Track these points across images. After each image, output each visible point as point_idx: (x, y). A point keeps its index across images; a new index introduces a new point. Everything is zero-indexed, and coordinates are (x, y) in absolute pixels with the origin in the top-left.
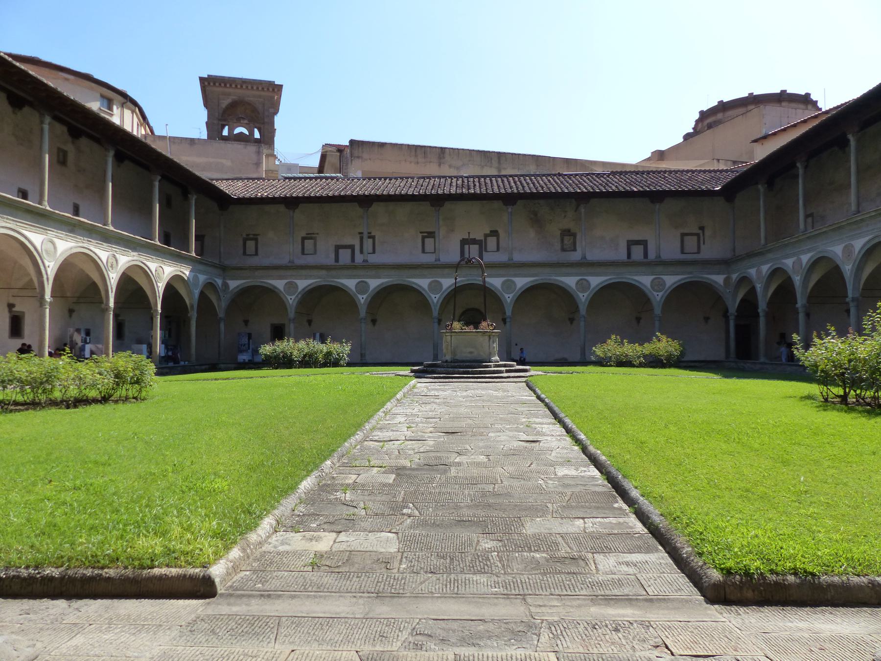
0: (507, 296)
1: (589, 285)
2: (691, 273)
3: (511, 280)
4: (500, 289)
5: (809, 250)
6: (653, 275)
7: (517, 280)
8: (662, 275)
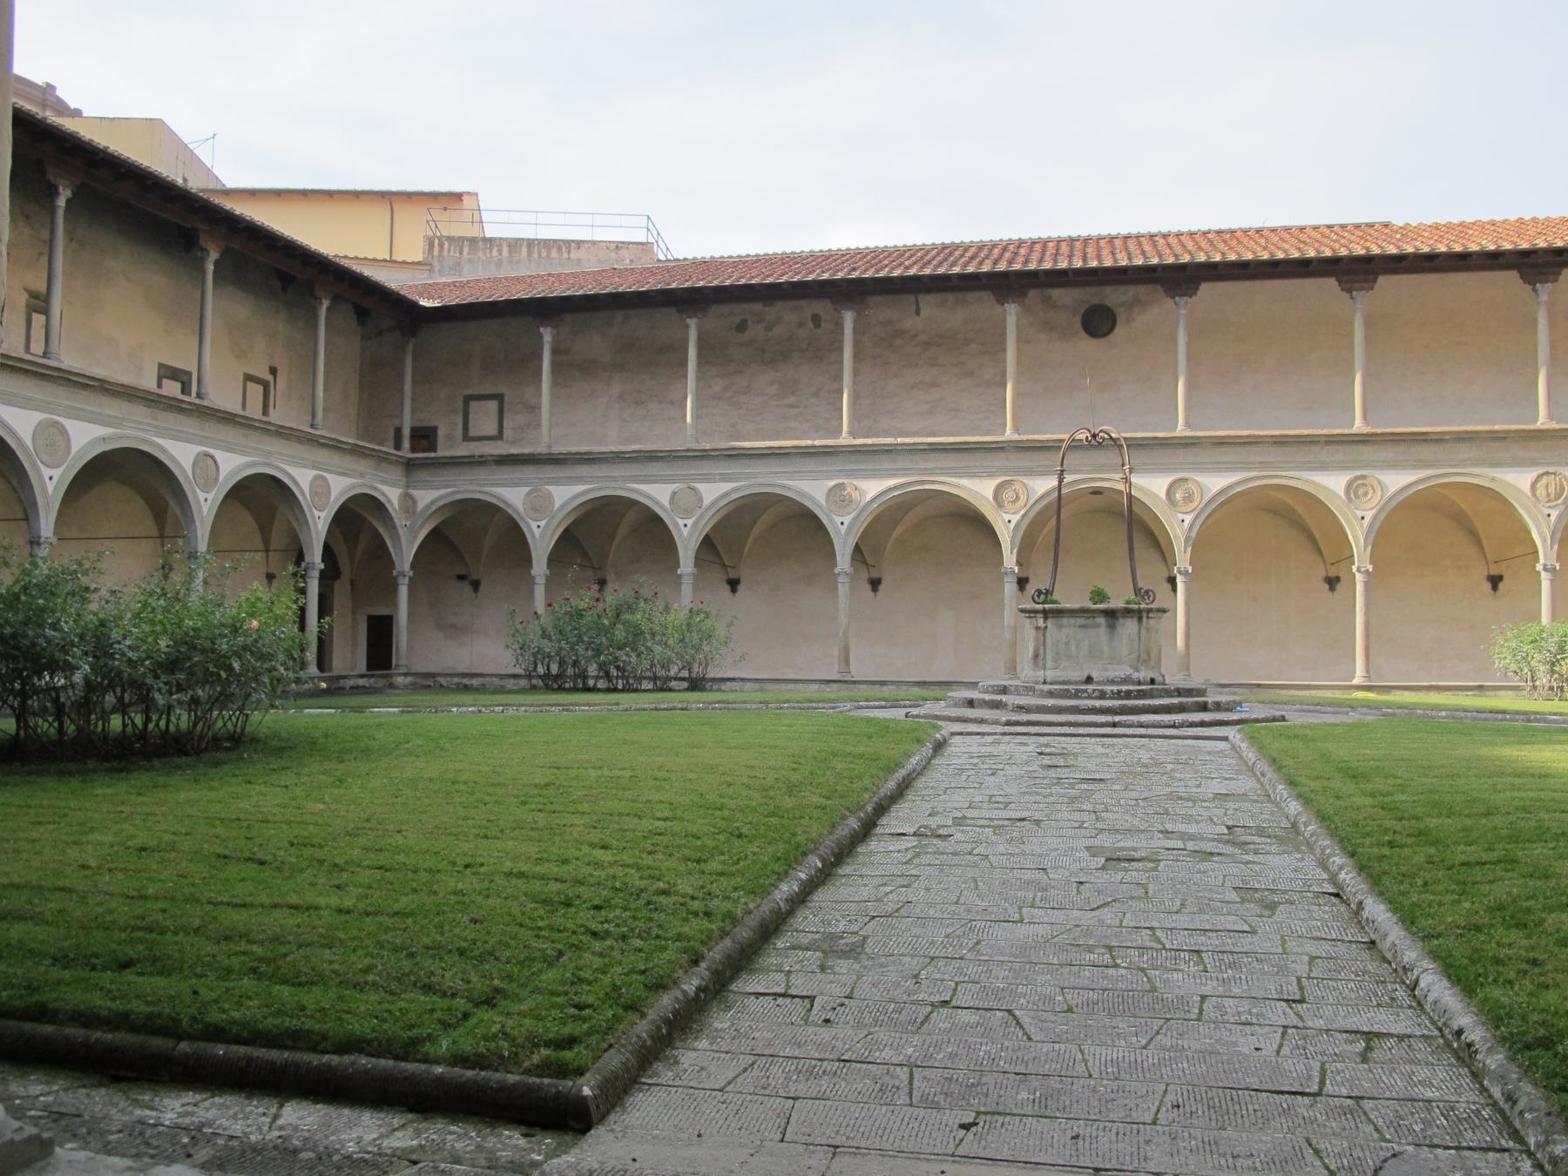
0: (46, 472)
1: (218, 469)
2: (362, 475)
3: (57, 423)
4: (29, 443)
5: (725, 478)
6: (314, 467)
7: (71, 425)
8: (330, 472)
